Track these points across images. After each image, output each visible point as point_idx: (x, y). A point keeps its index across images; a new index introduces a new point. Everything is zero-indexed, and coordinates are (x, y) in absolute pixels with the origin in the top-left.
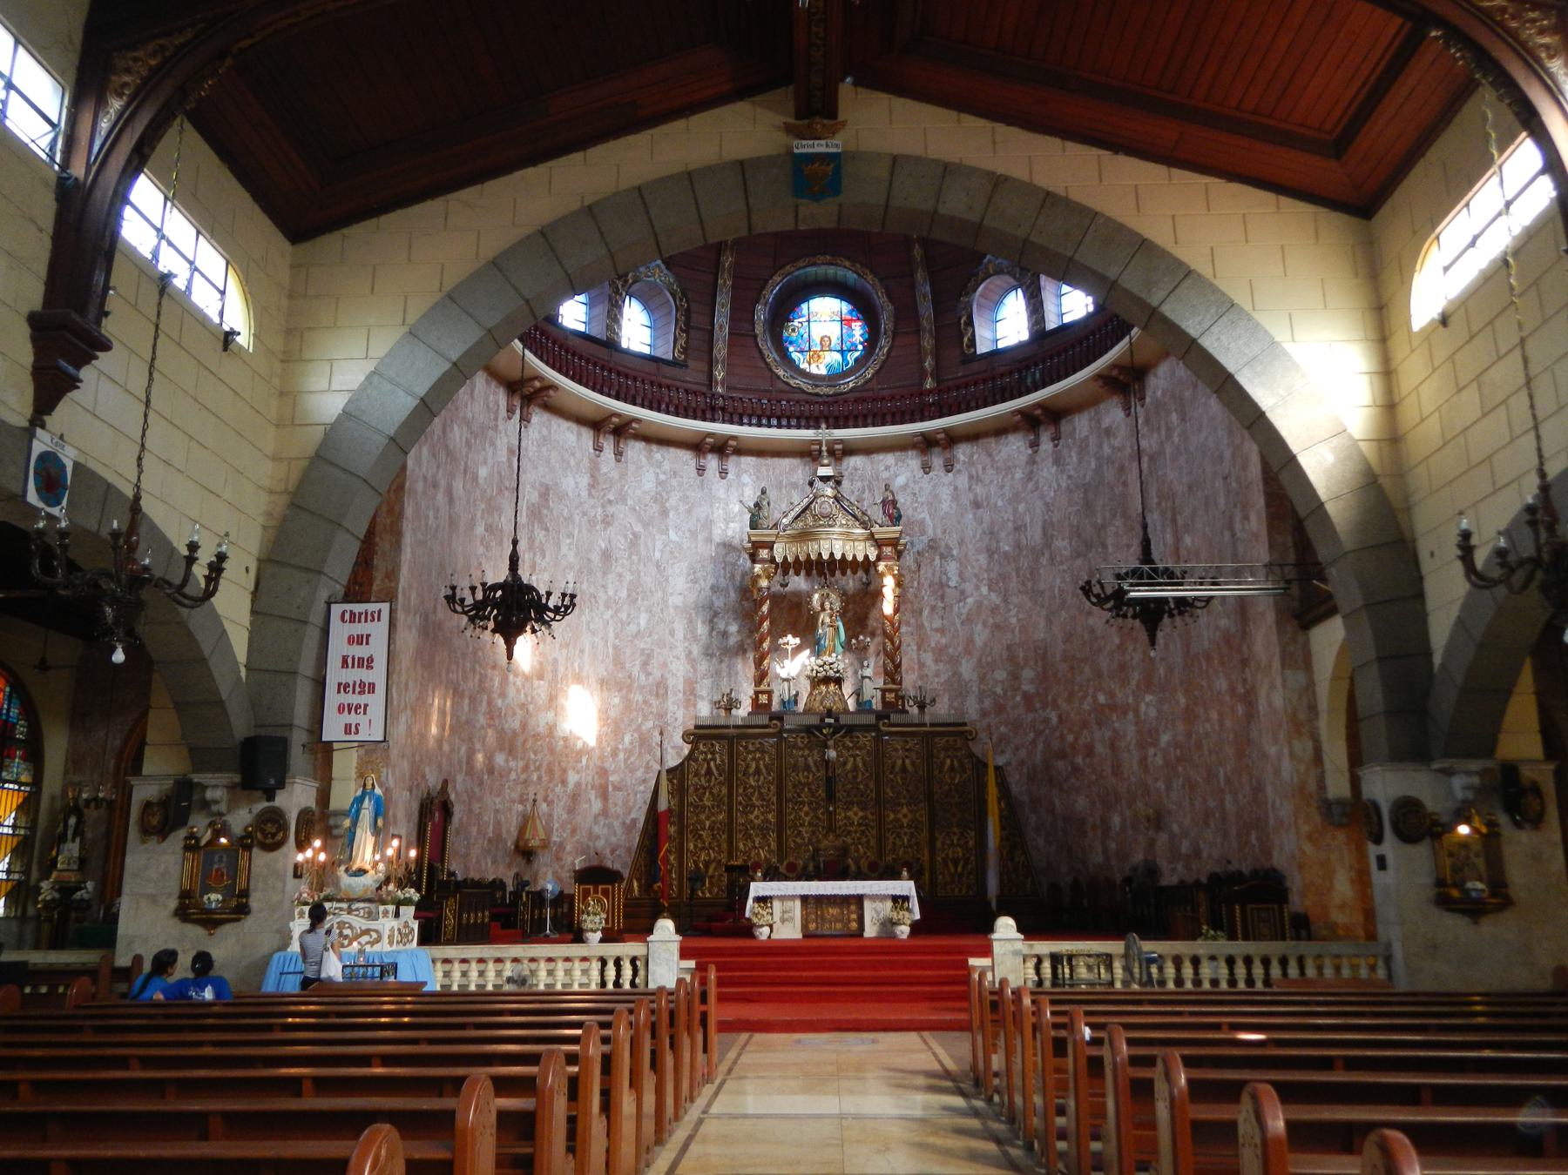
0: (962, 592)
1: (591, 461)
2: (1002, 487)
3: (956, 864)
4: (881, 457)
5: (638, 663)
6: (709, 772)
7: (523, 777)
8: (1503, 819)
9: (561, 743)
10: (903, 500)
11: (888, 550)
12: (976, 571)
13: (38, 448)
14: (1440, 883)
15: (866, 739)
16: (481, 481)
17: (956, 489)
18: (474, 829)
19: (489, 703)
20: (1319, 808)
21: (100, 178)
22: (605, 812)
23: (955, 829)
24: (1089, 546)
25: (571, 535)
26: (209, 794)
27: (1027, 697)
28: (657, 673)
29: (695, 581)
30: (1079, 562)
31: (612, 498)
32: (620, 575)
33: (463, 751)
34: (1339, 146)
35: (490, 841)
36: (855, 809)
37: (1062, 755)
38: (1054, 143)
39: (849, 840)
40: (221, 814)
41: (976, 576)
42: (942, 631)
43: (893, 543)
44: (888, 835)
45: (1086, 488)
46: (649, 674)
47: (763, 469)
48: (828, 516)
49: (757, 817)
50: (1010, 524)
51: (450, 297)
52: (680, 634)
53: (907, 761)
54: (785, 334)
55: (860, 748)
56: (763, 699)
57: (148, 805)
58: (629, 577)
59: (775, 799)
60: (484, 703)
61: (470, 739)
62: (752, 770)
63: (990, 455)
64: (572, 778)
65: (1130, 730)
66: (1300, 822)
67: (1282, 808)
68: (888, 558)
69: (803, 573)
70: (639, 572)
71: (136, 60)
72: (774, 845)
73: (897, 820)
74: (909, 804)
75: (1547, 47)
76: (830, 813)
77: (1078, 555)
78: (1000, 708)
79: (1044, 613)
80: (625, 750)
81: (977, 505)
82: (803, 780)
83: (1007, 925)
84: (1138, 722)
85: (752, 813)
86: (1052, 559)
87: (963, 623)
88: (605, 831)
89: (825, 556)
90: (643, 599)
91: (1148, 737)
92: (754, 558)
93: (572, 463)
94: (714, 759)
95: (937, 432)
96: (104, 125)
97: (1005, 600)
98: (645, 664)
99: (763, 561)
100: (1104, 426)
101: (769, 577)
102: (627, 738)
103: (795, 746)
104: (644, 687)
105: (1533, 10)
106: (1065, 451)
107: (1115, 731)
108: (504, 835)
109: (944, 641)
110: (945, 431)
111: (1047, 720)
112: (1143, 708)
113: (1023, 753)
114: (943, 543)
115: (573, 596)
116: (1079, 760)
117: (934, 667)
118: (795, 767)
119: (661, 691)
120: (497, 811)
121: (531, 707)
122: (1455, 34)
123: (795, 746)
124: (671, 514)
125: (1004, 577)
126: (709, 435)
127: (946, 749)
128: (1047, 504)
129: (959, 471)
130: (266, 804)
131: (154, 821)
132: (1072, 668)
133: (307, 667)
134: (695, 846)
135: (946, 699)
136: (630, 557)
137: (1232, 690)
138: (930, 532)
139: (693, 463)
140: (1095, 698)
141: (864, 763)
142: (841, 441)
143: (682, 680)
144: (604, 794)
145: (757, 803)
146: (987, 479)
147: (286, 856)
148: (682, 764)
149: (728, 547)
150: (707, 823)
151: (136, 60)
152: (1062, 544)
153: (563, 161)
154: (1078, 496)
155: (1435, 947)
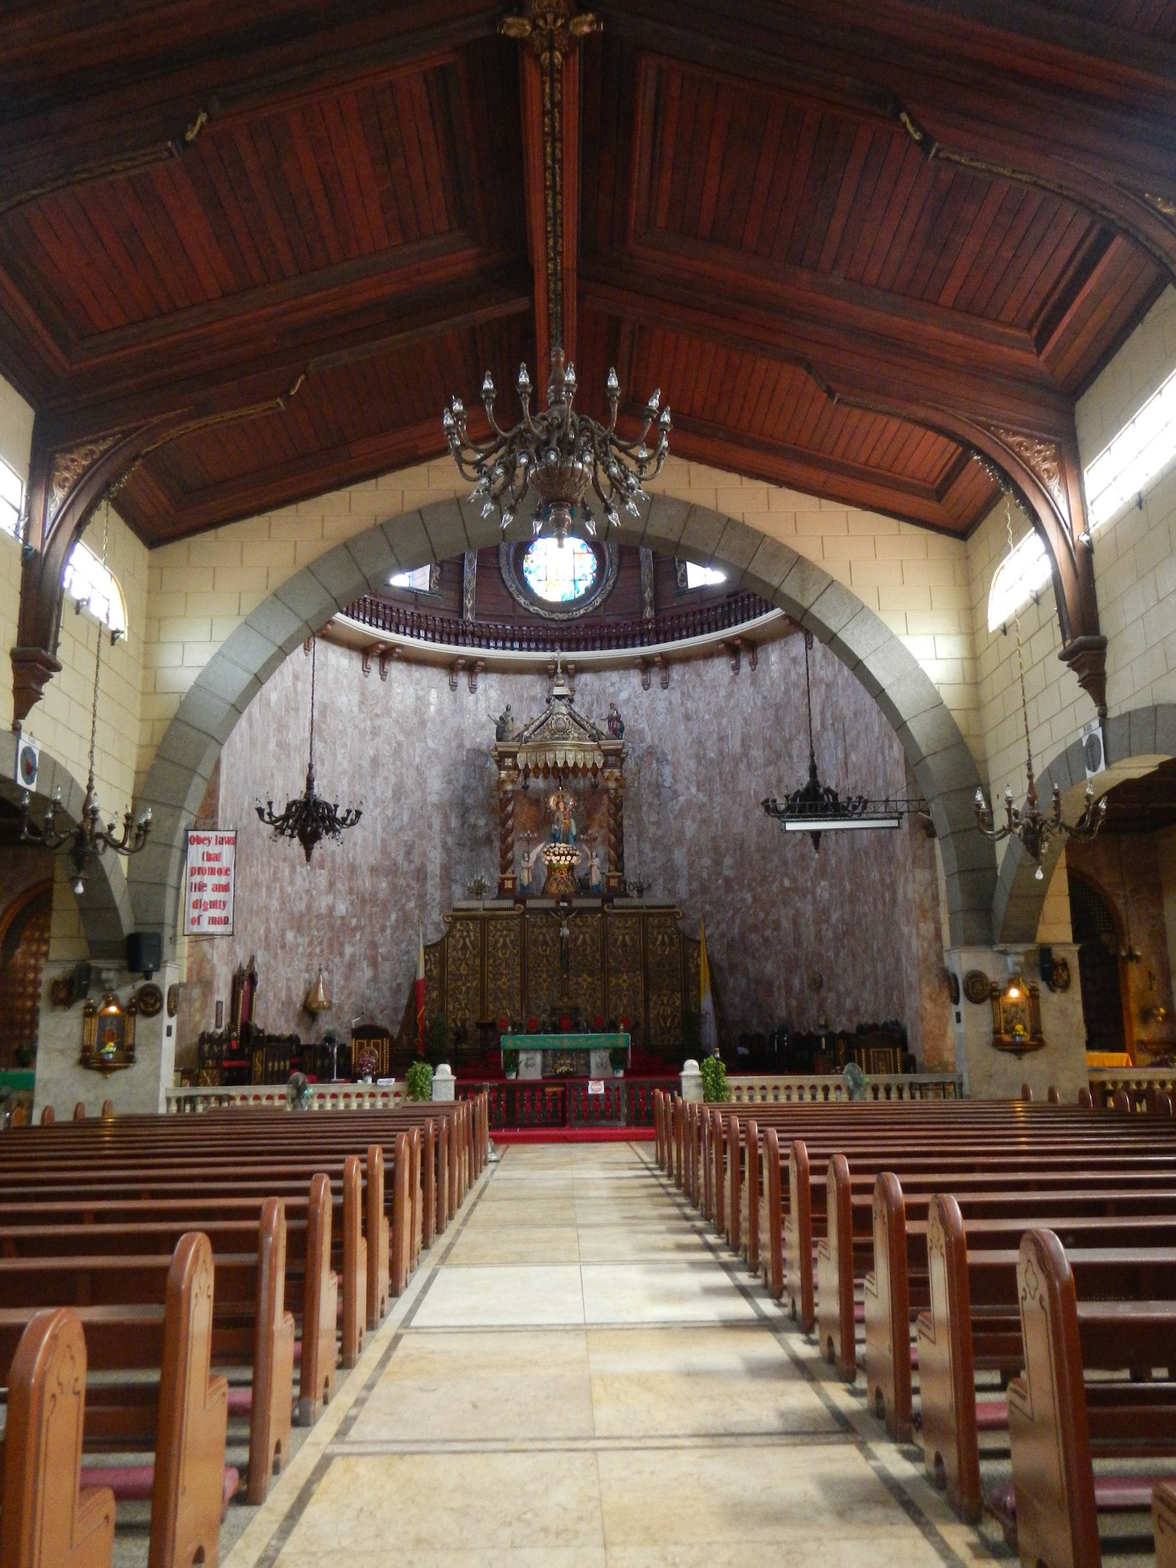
0: (675, 792)
1: (361, 681)
2: (709, 703)
3: (665, 1019)
4: (608, 674)
5: (402, 852)
6: (465, 946)
7: (309, 950)
8: (1042, 986)
9: (339, 921)
10: (625, 712)
11: (612, 759)
12: (686, 774)
13: (22, 745)
14: (996, 1031)
15: (594, 920)
16: (272, 705)
17: (670, 703)
18: (271, 995)
19: (281, 890)
20: (937, 975)
21: (53, 550)
22: (375, 979)
24: (779, 757)
25: (344, 746)
26: (104, 975)
27: (727, 880)
28: (418, 861)
29: (450, 782)
30: (771, 769)
31: (379, 712)
32: (386, 778)
33: (262, 931)
34: (939, 493)
35: (283, 1004)
37: (755, 928)
38: (734, 478)
40: (111, 990)
41: (686, 778)
42: (658, 824)
43: (617, 753)
45: (777, 707)
46: (411, 862)
47: (507, 685)
48: (564, 730)
49: (504, 983)
50: (715, 735)
51: (275, 595)
52: (437, 827)
53: (627, 937)
54: (525, 565)
55: (588, 927)
56: (509, 884)
57: (55, 984)
58: (393, 779)
60: (278, 891)
61: (267, 920)
62: (500, 945)
63: (699, 675)
64: (348, 950)
65: (808, 909)
66: (923, 986)
67: (911, 974)
68: (614, 766)
69: (541, 776)
70: (401, 775)
71: (73, 460)
72: (518, 1005)
73: (618, 985)
75: (1046, 470)
77: (769, 762)
78: (705, 890)
79: (741, 811)
80: (392, 927)
81: (688, 718)
83: (693, 1066)
84: (815, 902)
86: (749, 765)
87: (675, 818)
88: (376, 994)
89: (560, 764)
90: (406, 798)
91: (822, 915)
92: (501, 767)
93: (345, 683)
94: (469, 936)
95: (655, 655)
96: (53, 509)
97: (711, 799)
98: (408, 853)
99: (508, 768)
100: (792, 655)
101: (513, 782)
102: (393, 917)
103: (534, 926)
104: (406, 873)
105: (1040, 444)
106: (761, 675)
107: (797, 910)
108: (294, 999)
109: (660, 832)
110: (661, 655)
111: (743, 900)
112: (818, 891)
113: (723, 927)
114: (659, 750)
115: (358, 813)
116: (768, 933)
117: (651, 855)
118: (535, 942)
119: (421, 876)
120: (288, 979)
121: (314, 892)
122: (988, 459)
123: (534, 926)
124: (429, 725)
125: (710, 780)
126: (461, 657)
127: (659, 927)
128: (745, 719)
129: (673, 688)
130: (146, 982)
131: (62, 995)
132: (764, 858)
133: (172, 880)
135: (661, 881)
136: (394, 762)
137: (882, 880)
138: (649, 739)
139: (446, 679)
140: (782, 882)
141: (592, 939)
142: (573, 662)
143: (438, 867)
144: (374, 964)
146: (696, 695)
147: (162, 1020)
148: (442, 940)
149: (477, 752)
150: (464, 989)
151: (73, 460)
152: (757, 753)
153: (361, 486)
154: (771, 713)
155: (991, 1076)
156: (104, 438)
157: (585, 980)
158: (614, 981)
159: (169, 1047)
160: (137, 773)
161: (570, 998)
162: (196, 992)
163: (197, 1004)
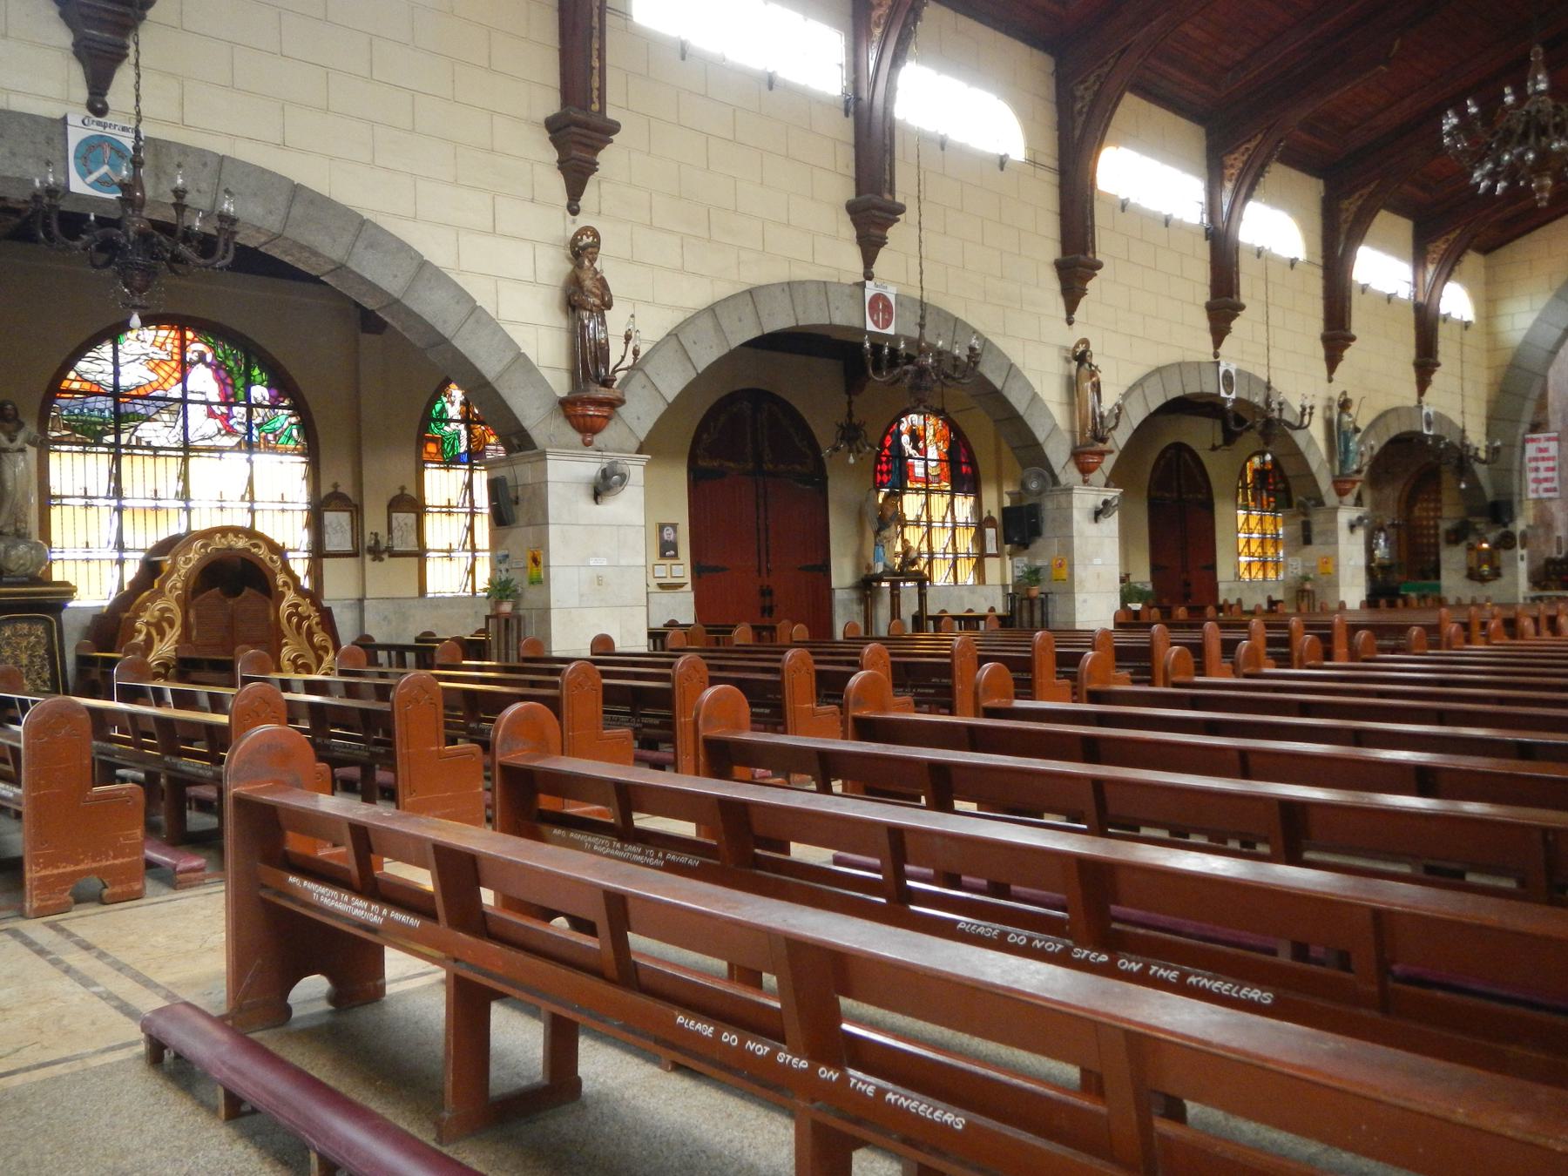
26: (1478, 526)
40: (1483, 534)
57: (1448, 533)
96: (1428, 278)
131: (1453, 538)
133: (1516, 465)
156: (1454, 230)
159: (1523, 568)
160: (1488, 402)
162: (1541, 531)
163: (1542, 539)
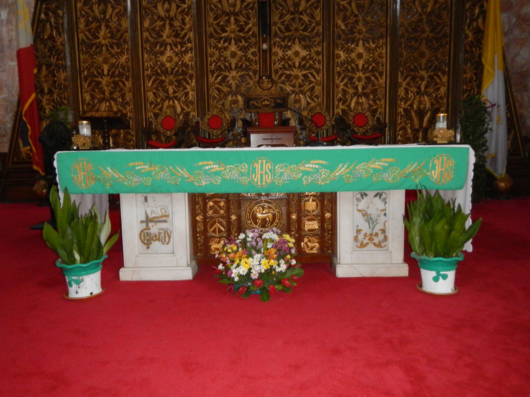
23: (423, 73)
36: (297, 47)
39: (289, 89)
44: (337, 81)
49: (170, 60)
59: (191, 35)
72: (192, 95)
74: (366, 41)
76: (265, 51)
82: (227, 9)
85: (162, 53)
134: (93, 97)
145: (169, 41)
150: (106, 68)
157: (297, 54)
158: (343, 55)
161: (273, 82)
